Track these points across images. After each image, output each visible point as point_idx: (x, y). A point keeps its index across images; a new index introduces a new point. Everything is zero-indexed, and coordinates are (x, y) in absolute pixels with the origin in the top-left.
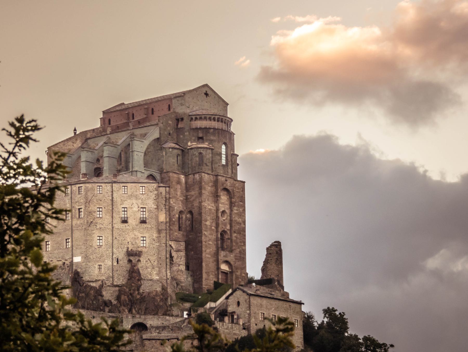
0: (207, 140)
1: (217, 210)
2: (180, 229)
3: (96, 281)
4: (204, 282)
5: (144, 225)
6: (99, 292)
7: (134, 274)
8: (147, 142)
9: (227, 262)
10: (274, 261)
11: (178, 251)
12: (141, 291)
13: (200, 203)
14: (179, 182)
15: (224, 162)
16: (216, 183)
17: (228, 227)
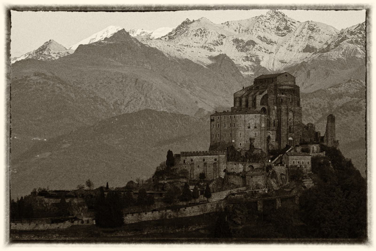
0: (284, 94)
1: (288, 119)
2: (274, 126)
3: (239, 149)
4: (282, 145)
5: (256, 129)
6: (240, 153)
7: (252, 147)
8: (262, 96)
9: (292, 137)
10: (330, 122)
11: (272, 134)
12: (254, 153)
13: (281, 117)
14: (274, 109)
15: (291, 101)
16: (287, 109)
17: (292, 124)
